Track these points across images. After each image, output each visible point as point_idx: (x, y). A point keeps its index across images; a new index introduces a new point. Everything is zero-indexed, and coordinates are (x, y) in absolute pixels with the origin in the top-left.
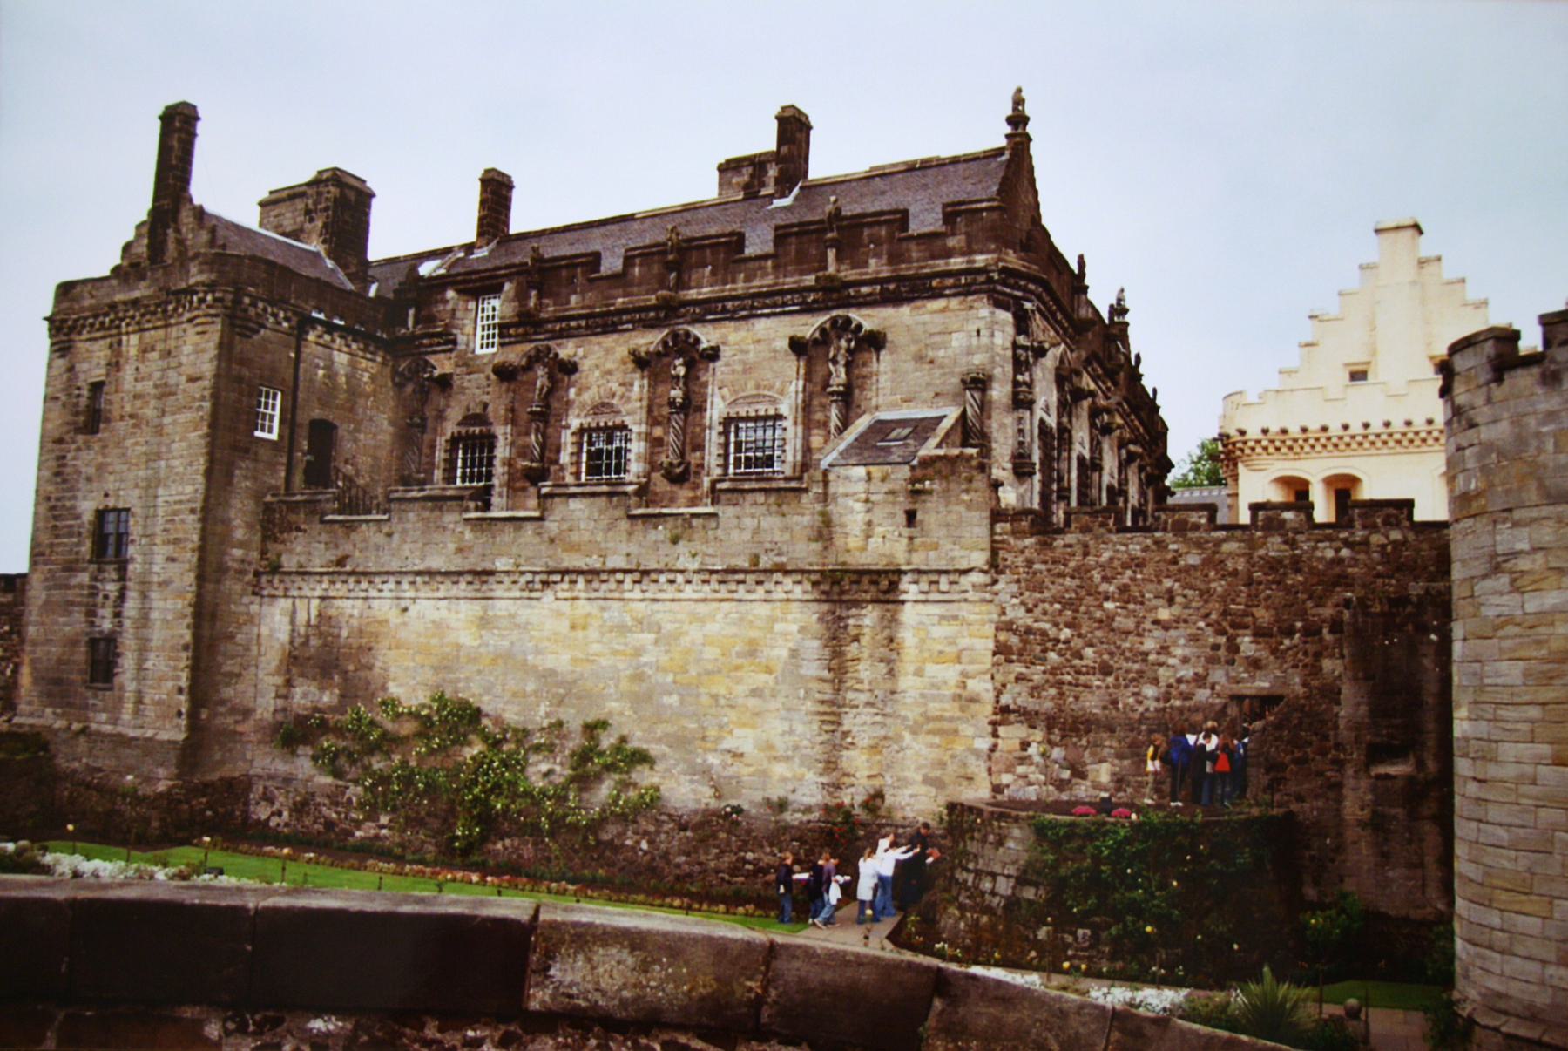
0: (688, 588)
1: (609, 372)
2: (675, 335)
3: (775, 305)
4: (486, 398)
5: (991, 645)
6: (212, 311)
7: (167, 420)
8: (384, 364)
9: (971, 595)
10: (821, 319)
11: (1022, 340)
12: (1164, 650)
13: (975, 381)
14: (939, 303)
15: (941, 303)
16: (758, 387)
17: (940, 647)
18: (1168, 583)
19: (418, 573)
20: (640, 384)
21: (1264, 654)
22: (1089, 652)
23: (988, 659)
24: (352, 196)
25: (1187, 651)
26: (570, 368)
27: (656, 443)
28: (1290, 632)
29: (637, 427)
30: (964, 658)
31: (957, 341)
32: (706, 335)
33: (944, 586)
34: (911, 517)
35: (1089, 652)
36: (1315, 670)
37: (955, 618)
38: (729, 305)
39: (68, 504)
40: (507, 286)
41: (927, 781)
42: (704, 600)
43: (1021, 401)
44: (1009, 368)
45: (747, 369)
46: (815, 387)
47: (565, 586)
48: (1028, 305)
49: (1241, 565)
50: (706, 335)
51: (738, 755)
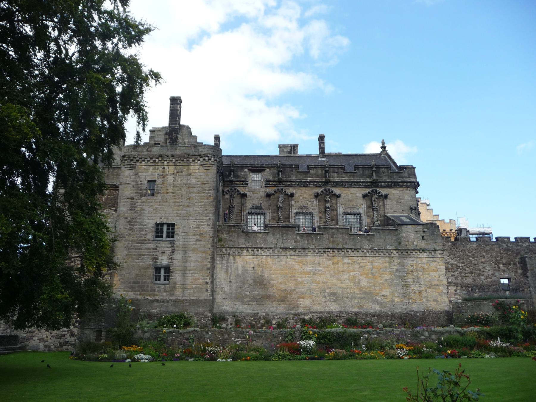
0: (368, 254)
2: (325, 190)
5: (444, 268)
6: (213, 163)
9: (439, 256)
12: (484, 268)
15: (401, 189)
16: (353, 205)
18: (483, 254)
19: (282, 248)
21: (506, 269)
22: (467, 269)
23: (444, 271)
25: (489, 268)
27: (320, 218)
28: (510, 264)
32: (337, 191)
33: (433, 254)
34: (423, 237)
35: (467, 269)
36: (516, 272)
38: (344, 183)
39: (138, 220)
41: (434, 300)
45: (350, 201)
46: (370, 206)
47: (332, 252)
49: (498, 250)
50: (337, 191)
51: (384, 296)
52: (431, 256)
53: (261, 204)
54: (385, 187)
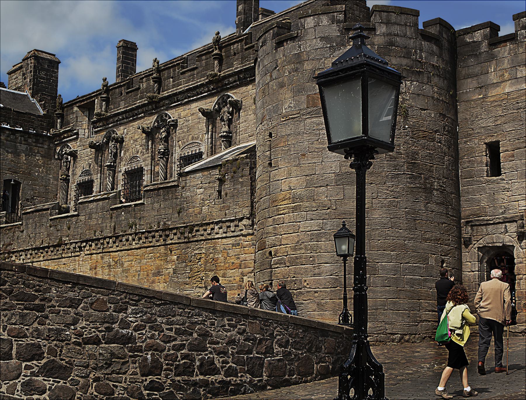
1: (136, 141)
9: (244, 232)
10: (216, 99)
17: (232, 261)
26: (120, 141)
30: (243, 266)
34: (220, 192)
37: (238, 244)
38: (180, 97)
40: (96, 100)
42: (140, 248)
50: (173, 114)
52: (230, 234)
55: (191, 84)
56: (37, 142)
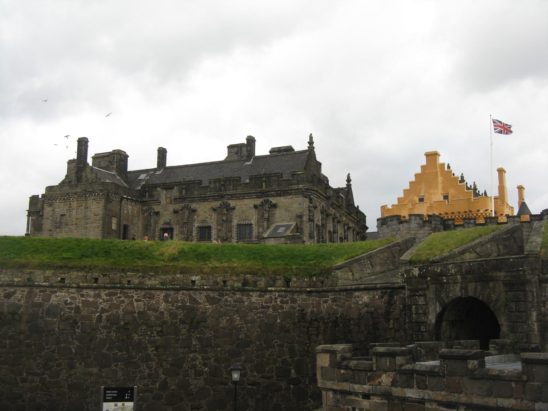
1: (206, 212)
3: (250, 196)
4: (170, 218)
7: (88, 226)
8: (139, 208)
10: (262, 200)
11: (311, 205)
13: (299, 216)
14: (291, 196)
16: (246, 216)
20: (214, 216)
24: (123, 158)
27: (219, 230)
29: (214, 226)
31: (295, 206)
32: (232, 203)
38: (238, 196)
40: (175, 188)
43: (311, 220)
44: (308, 212)
45: (243, 212)
48: (312, 197)
50: (232, 203)
53: (170, 220)
54: (275, 196)
55: (246, 191)
56: (135, 204)
